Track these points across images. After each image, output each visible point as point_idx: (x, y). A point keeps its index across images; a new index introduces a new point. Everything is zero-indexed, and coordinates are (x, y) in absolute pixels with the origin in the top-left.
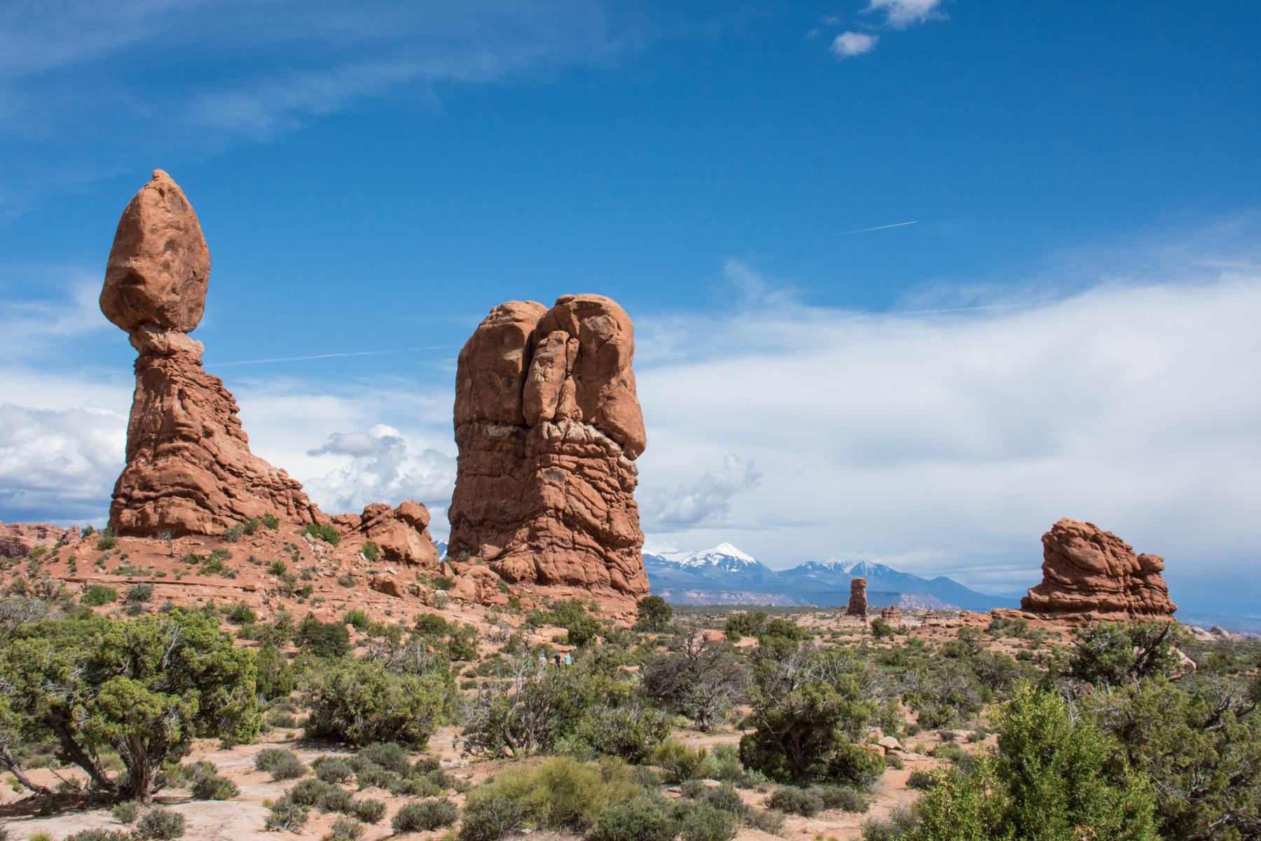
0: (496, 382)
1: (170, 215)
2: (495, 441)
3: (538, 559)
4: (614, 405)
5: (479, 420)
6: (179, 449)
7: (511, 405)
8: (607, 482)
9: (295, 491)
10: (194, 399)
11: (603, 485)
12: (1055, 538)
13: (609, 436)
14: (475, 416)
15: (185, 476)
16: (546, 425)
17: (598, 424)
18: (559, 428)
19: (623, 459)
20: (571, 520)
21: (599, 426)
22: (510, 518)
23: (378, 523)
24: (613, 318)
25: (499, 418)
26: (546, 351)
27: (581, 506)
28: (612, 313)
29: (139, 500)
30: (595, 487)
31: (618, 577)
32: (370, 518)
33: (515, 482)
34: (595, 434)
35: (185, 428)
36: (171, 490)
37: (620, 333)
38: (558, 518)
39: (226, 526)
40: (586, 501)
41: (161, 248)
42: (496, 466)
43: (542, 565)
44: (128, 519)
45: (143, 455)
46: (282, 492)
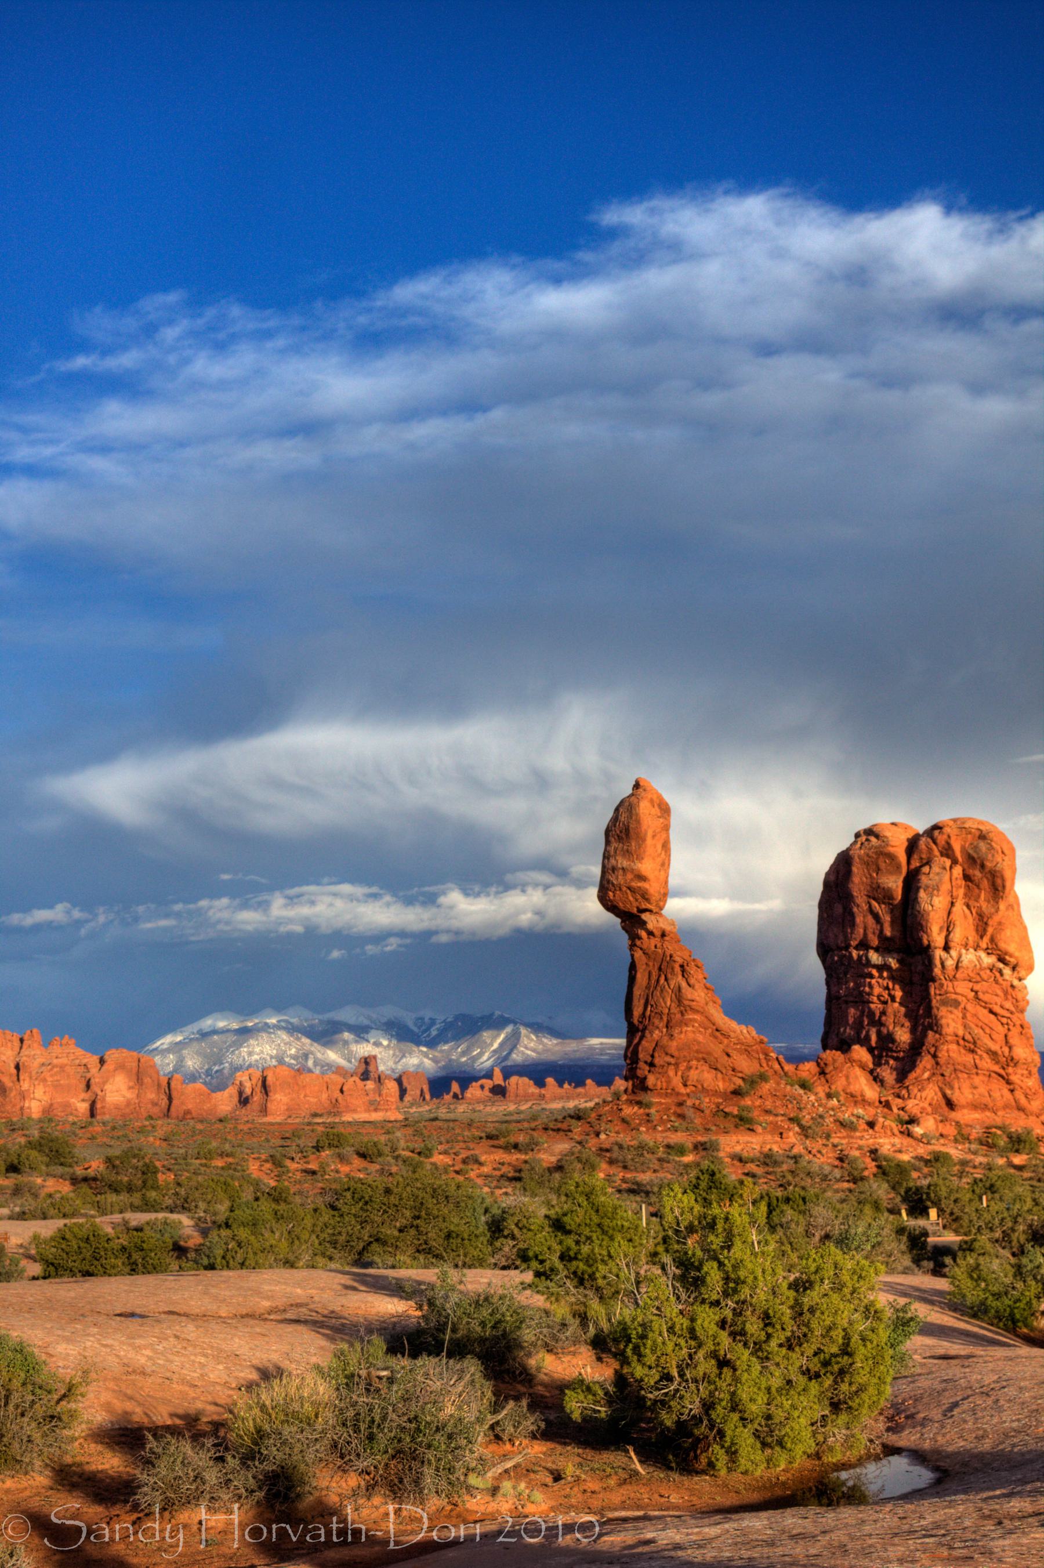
1: (661, 820)
6: (691, 1020)
8: (1002, 1007)
11: (997, 1009)
15: (699, 1043)
16: (939, 954)
19: (1016, 982)
23: (835, 1069)
30: (991, 1012)
31: (1023, 1101)
34: (988, 960)
37: (1006, 858)
38: (958, 1044)
43: (948, 1092)
45: (658, 1028)
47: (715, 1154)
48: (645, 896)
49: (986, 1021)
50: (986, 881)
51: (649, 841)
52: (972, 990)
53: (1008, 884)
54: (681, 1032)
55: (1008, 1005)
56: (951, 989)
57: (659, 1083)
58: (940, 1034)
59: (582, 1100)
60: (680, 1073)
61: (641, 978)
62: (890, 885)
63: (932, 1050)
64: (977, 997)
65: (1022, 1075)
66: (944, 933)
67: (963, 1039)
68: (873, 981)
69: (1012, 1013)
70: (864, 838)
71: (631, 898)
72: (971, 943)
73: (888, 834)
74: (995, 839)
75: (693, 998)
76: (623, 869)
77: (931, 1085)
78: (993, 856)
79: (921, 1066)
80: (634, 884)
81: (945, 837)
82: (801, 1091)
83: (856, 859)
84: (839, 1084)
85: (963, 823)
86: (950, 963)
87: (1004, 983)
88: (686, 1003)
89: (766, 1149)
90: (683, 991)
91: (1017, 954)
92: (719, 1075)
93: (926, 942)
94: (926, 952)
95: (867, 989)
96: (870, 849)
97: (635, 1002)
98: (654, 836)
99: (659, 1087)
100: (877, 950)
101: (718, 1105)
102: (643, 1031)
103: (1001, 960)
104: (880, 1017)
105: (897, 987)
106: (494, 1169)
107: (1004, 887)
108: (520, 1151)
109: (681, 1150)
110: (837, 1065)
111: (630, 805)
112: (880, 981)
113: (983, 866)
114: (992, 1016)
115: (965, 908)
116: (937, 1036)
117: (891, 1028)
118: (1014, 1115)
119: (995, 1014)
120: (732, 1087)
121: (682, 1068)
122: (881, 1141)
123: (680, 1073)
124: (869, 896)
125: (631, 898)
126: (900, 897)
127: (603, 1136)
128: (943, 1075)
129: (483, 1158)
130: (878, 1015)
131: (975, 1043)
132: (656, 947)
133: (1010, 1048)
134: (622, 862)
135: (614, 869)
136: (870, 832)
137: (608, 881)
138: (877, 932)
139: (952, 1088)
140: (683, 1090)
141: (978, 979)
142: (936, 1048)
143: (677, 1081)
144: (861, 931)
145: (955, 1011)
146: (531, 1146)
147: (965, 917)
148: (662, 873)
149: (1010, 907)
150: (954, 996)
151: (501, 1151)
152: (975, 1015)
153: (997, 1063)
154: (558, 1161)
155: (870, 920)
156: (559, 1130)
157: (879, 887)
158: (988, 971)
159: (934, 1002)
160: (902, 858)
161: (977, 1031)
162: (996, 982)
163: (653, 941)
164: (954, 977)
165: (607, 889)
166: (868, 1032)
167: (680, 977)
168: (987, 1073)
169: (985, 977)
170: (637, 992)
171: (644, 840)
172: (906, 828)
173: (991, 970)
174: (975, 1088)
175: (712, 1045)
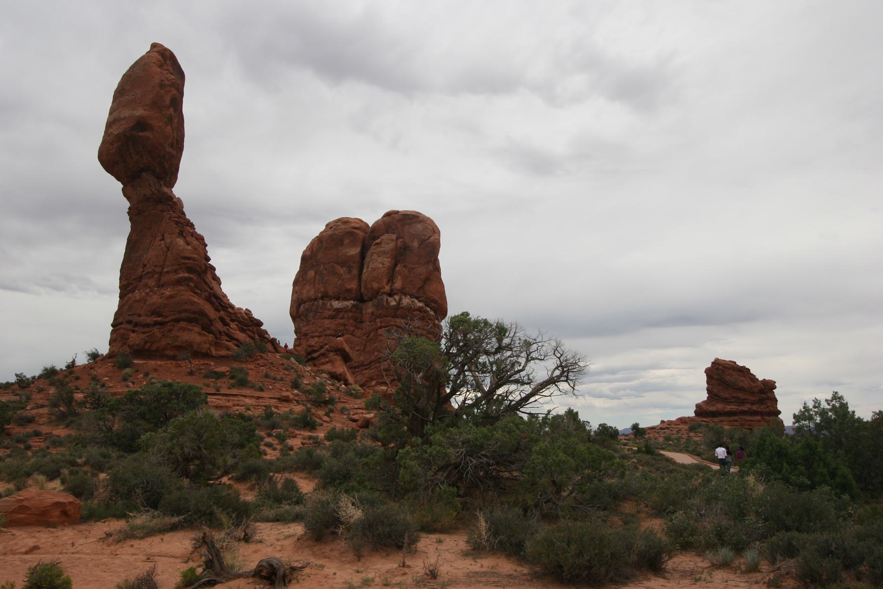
0: (338, 271)
1: (173, 77)
2: (338, 311)
5: (322, 298)
7: (353, 285)
9: (258, 328)
10: (196, 236)
12: (714, 370)
13: (427, 305)
14: (320, 295)
17: (419, 297)
18: (395, 300)
19: (437, 322)
21: (421, 299)
22: (357, 364)
24: (429, 225)
25: (341, 296)
26: (382, 247)
28: (428, 222)
29: (148, 325)
32: (314, 351)
33: (357, 339)
34: (421, 304)
35: (191, 261)
36: (178, 316)
41: (168, 102)
42: (340, 328)
44: (137, 342)
46: (250, 328)
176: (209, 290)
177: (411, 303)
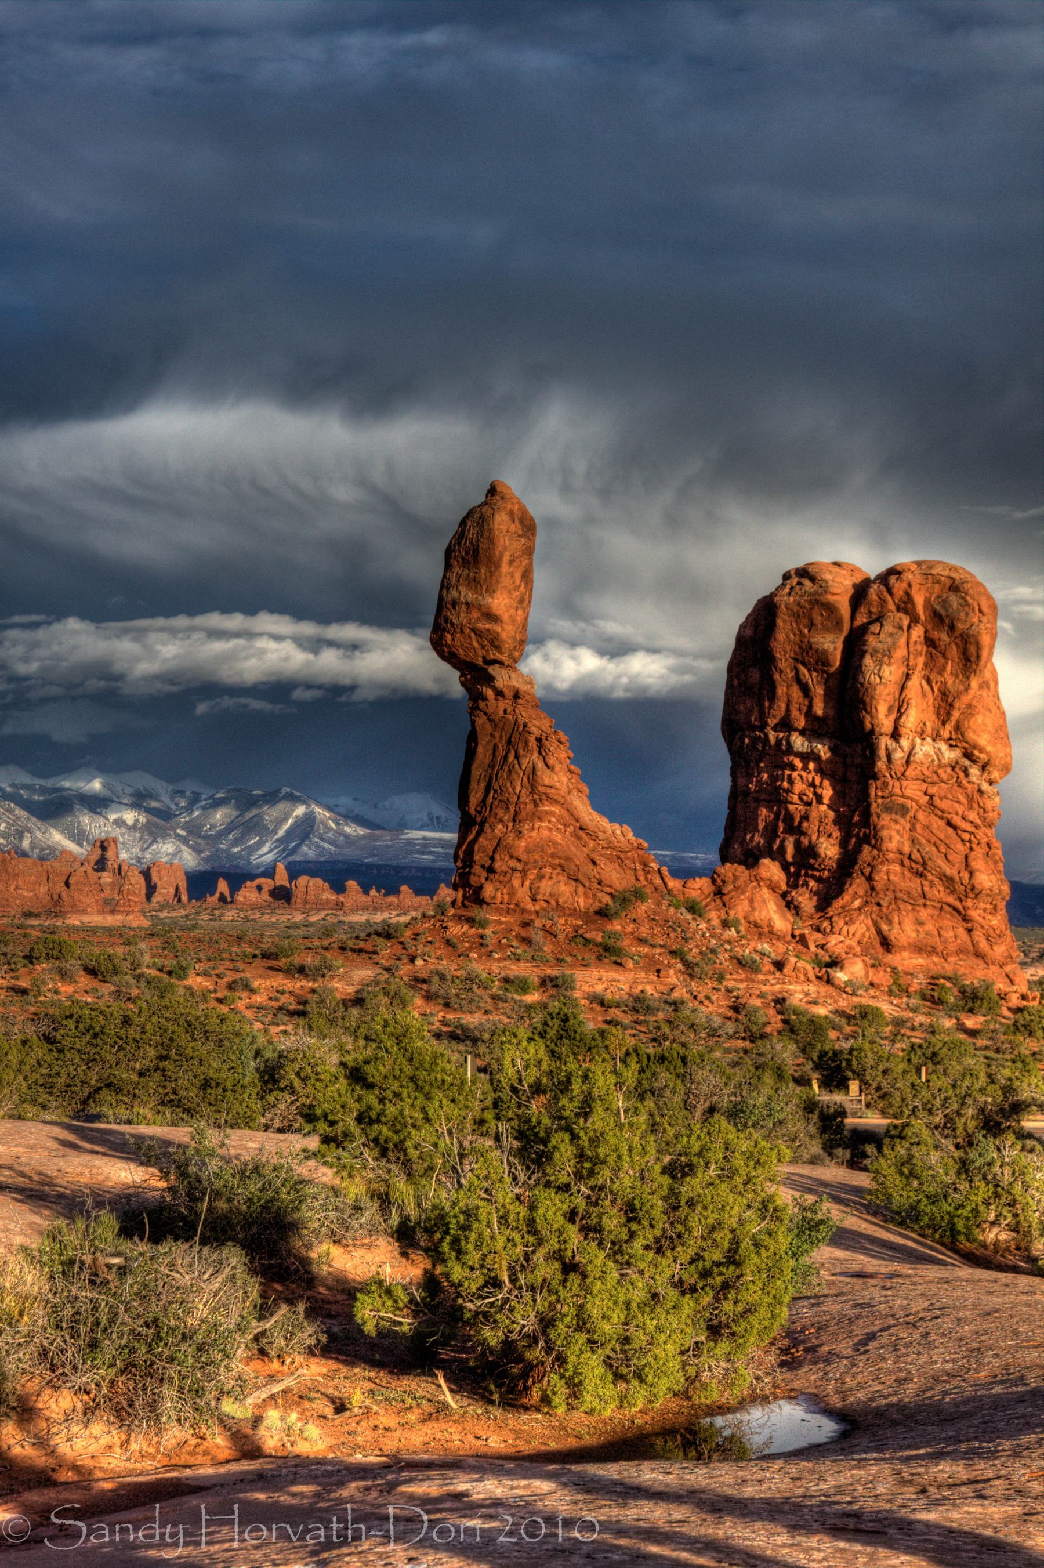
1: (523, 540)
3: (879, 920)
4: (973, 715)
6: (546, 813)
8: (964, 817)
9: (641, 852)
11: (957, 820)
15: (555, 844)
16: (884, 742)
19: (985, 786)
20: (919, 869)
27: (934, 848)
30: (949, 823)
31: (983, 945)
34: (950, 755)
35: (553, 791)
37: (985, 619)
38: (902, 864)
39: (600, 901)
40: (938, 842)
41: (518, 582)
43: (885, 928)
45: (501, 821)
47: (569, 993)
48: (495, 642)
49: (942, 836)
50: (954, 647)
51: (505, 568)
52: (926, 794)
53: (984, 653)
54: (533, 829)
55: (972, 816)
56: (897, 791)
57: (499, 895)
58: (879, 850)
59: (394, 913)
60: (527, 883)
61: (483, 752)
62: (826, 646)
63: (867, 871)
64: (931, 804)
65: (985, 910)
66: (893, 716)
67: (910, 858)
68: (795, 774)
69: (977, 827)
70: (795, 580)
71: (475, 644)
72: (929, 730)
73: (828, 577)
74: (971, 592)
75: (551, 783)
76: (467, 604)
77: (862, 917)
78: (967, 614)
79: (851, 891)
80: (480, 625)
81: (904, 585)
82: (689, 917)
83: (783, 607)
84: (740, 909)
85: (931, 568)
86: (899, 756)
87: (969, 786)
88: (542, 789)
89: (636, 991)
90: (539, 773)
91: (989, 748)
92: (581, 889)
93: (868, 726)
94: (867, 740)
95: (785, 784)
96: (801, 596)
97: (473, 784)
98: (511, 563)
99: (498, 900)
100: (802, 733)
101: (576, 929)
102: (482, 824)
103: (968, 755)
104: (800, 823)
105: (826, 783)
106: (270, 999)
107: (978, 657)
108: (306, 976)
109: (524, 987)
110: (738, 883)
111: (482, 517)
112: (804, 774)
113: (952, 628)
114: (950, 830)
115: (924, 683)
116: (875, 852)
117: (814, 838)
118: (969, 962)
119: (955, 828)
120: (597, 905)
121: (532, 877)
122: (791, 987)
123: (527, 883)
124: (796, 660)
125: (475, 644)
126: (838, 663)
127: (419, 962)
128: (879, 904)
129: (255, 984)
130: (797, 820)
131: (924, 864)
132: (505, 711)
133: (971, 874)
134: (466, 594)
135: (454, 603)
136: (803, 573)
137: (446, 620)
138: (805, 709)
139: (890, 922)
140: (530, 906)
141: (935, 778)
142: (873, 867)
143: (523, 894)
144: (783, 706)
145: (902, 821)
146: (322, 971)
147: (924, 695)
148: (520, 612)
149: (984, 685)
150: (901, 800)
151: (281, 975)
152: (927, 827)
153: (953, 892)
154: (358, 992)
155: (796, 692)
156: (360, 951)
157: (811, 648)
158: (949, 770)
159: (874, 806)
160: (845, 610)
161: (928, 848)
162: (960, 785)
163: (503, 704)
164: (903, 774)
165: (444, 630)
166: (783, 842)
167: (536, 754)
168: (939, 905)
169: (944, 777)
170: (476, 772)
171: (498, 566)
172: (853, 570)
173: (953, 769)
174: (921, 924)
175: (573, 849)
176: (574, 822)
177: (932, 753)
